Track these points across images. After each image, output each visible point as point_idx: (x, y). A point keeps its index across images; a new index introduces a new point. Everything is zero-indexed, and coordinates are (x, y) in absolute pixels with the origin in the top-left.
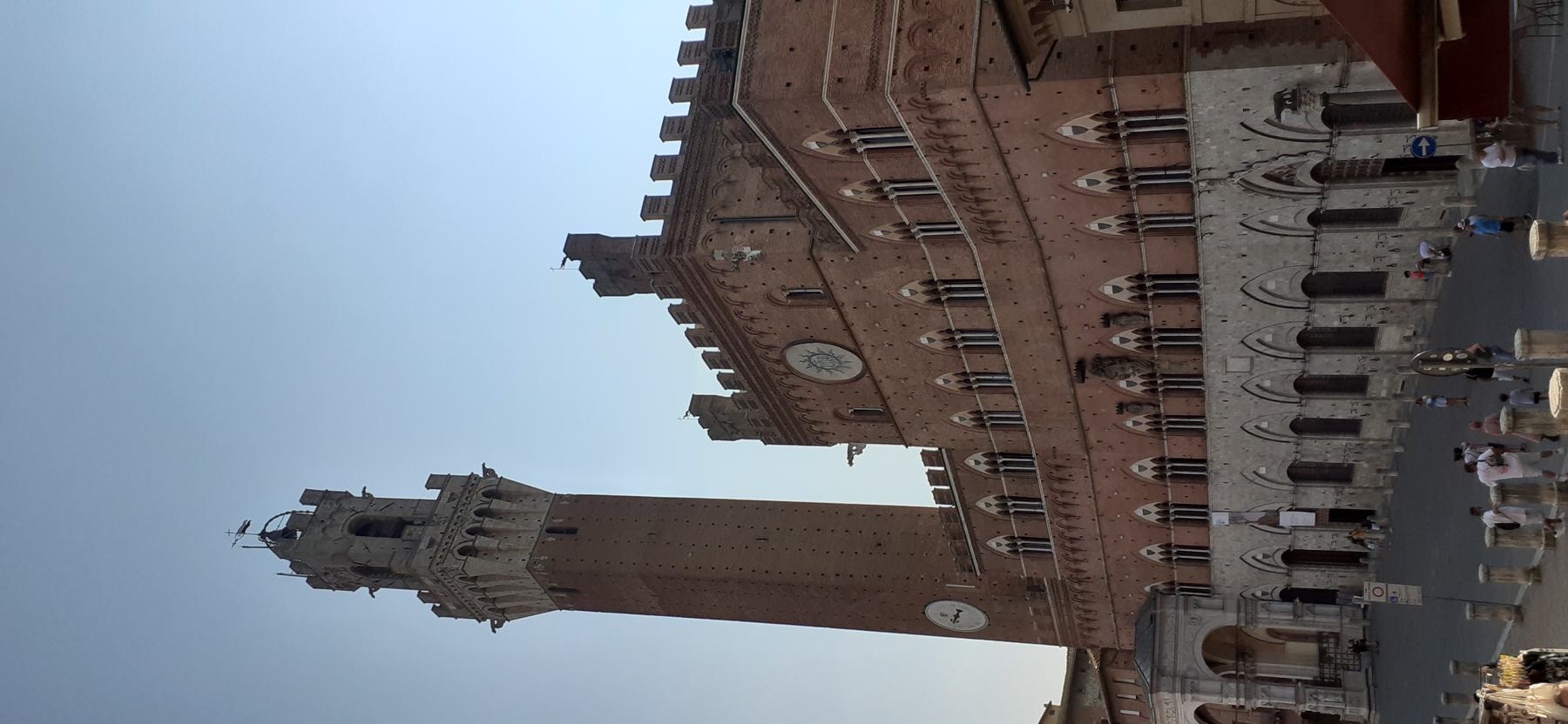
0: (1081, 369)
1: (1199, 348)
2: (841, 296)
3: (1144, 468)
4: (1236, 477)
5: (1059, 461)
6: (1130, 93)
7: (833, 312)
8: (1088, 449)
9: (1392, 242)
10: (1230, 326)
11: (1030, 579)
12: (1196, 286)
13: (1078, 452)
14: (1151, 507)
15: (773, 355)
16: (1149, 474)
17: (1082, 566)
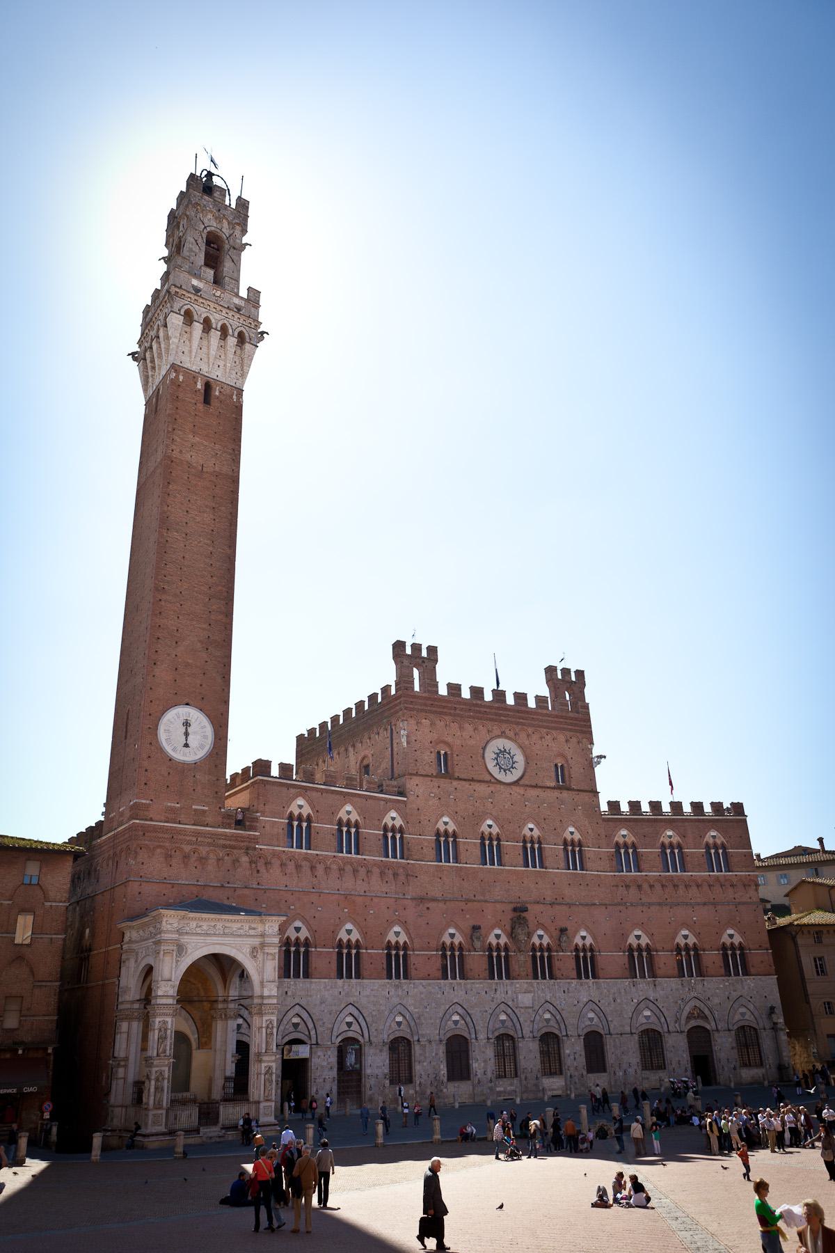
0: (520, 911)
1: (536, 977)
2: (565, 794)
3: (397, 935)
4: (395, 1000)
5: (402, 878)
6: (761, 956)
7: (553, 784)
8: (421, 900)
9: (631, 1071)
10: (560, 994)
11: (256, 820)
12: (587, 977)
13: (412, 891)
14: (355, 936)
15: (507, 732)
16: (391, 937)
17: (276, 870)
